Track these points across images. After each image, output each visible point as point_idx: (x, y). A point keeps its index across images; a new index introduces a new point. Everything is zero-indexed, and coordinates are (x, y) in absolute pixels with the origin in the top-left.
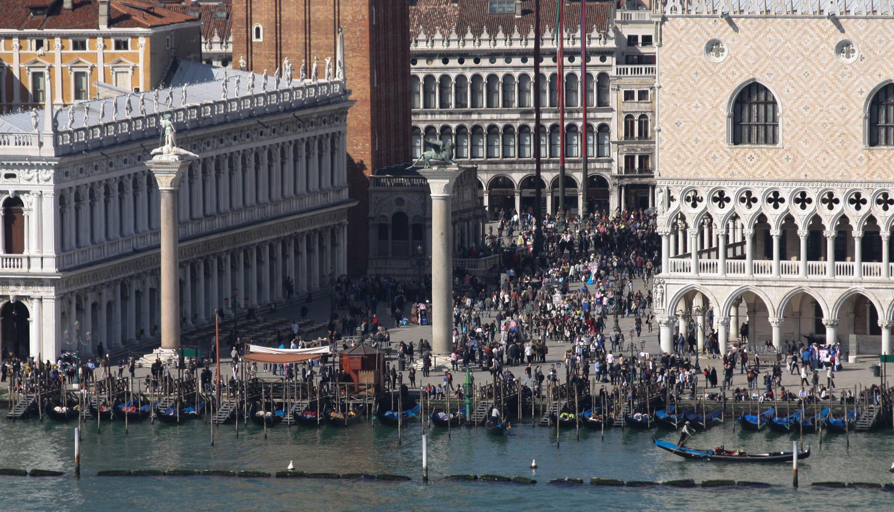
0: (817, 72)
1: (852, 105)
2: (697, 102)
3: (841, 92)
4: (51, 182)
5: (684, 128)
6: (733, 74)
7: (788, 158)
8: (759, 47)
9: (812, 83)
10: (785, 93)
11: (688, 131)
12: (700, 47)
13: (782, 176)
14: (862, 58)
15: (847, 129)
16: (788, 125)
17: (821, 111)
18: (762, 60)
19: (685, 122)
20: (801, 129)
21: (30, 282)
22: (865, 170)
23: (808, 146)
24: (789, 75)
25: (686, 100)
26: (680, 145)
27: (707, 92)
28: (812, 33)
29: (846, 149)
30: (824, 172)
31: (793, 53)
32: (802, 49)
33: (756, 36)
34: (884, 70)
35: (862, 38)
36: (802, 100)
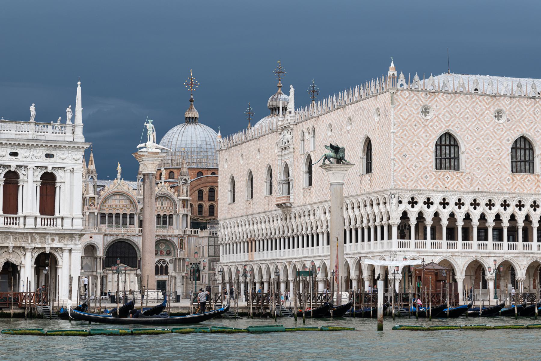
0: (484, 128)
1: (503, 147)
2: (416, 143)
3: (497, 140)
6: (437, 126)
7: (468, 178)
8: (451, 111)
9: (481, 134)
10: (466, 139)
11: (411, 161)
12: (418, 109)
13: (465, 189)
15: (501, 162)
16: (468, 158)
17: (486, 150)
18: (453, 119)
19: (409, 154)
20: (475, 161)
21: (63, 236)
22: (511, 186)
23: (479, 171)
25: (409, 141)
27: (422, 137)
28: (481, 104)
29: (500, 173)
30: (489, 187)
31: (470, 115)
33: (450, 105)
35: (508, 108)
36: (475, 144)
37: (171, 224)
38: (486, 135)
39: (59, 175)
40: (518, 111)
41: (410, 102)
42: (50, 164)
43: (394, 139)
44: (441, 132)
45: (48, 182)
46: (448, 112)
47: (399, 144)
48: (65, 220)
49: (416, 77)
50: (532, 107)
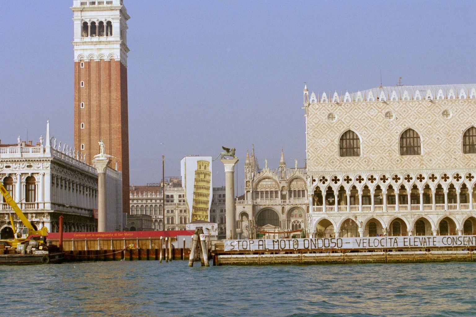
1: (393, 138)
2: (324, 139)
4: (49, 168)
5: (319, 150)
11: (321, 152)
14: (397, 118)
15: (391, 148)
21: (38, 214)
22: (400, 165)
23: (374, 156)
24: (365, 126)
25: (319, 139)
26: (317, 157)
28: (374, 108)
29: (391, 156)
32: (370, 116)
33: (350, 111)
34: (407, 123)
37: (304, 196)
38: (379, 130)
39: (36, 177)
40: (405, 111)
41: (319, 112)
42: (30, 171)
43: (308, 138)
44: (343, 130)
45: (30, 181)
46: (349, 117)
47: (311, 140)
48: (40, 205)
49: (336, 94)
50: (417, 107)
